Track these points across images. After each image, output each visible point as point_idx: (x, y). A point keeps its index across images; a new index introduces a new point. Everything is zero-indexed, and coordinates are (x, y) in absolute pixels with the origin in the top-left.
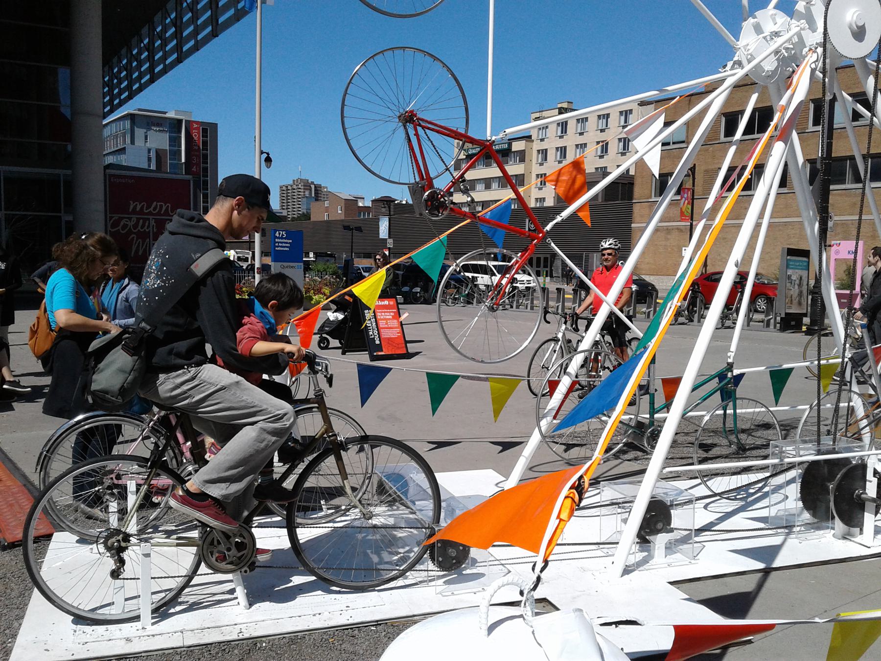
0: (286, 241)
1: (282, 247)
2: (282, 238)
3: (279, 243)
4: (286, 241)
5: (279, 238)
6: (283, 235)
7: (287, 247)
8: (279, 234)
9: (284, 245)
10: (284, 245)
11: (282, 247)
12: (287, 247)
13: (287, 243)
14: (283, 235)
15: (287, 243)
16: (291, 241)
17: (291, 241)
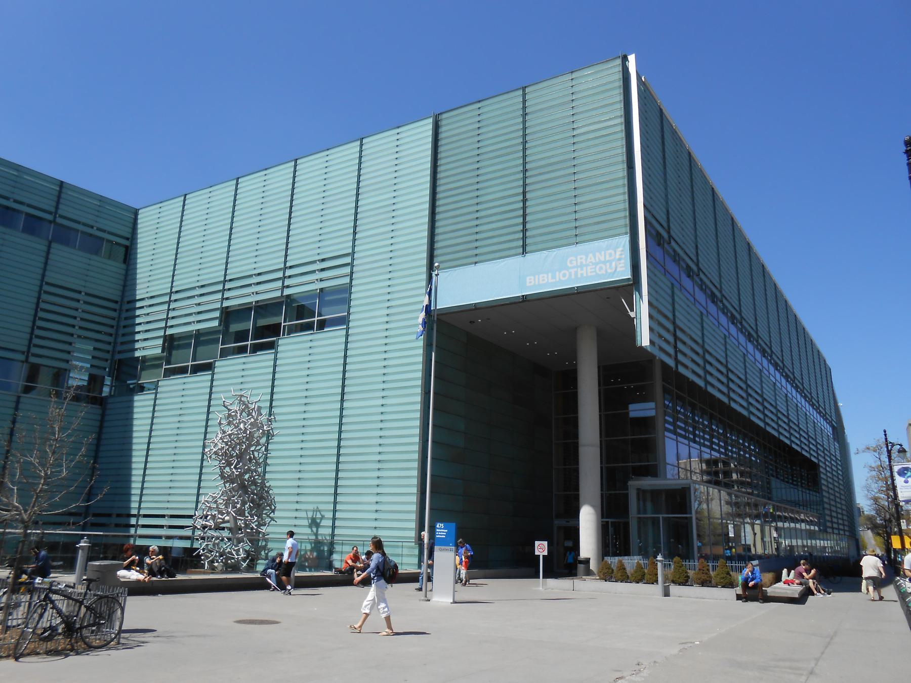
0: (443, 531)
1: (440, 535)
2: (441, 529)
3: (439, 532)
4: (443, 531)
5: (439, 529)
6: (441, 526)
7: (444, 535)
8: (439, 525)
9: (442, 533)
10: (442, 533)
11: (440, 535)
12: (444, 535)
13: (444, 532)
14: (441, 526)
15: (444, 532)
16: (447, 531)
17: (447, 531)
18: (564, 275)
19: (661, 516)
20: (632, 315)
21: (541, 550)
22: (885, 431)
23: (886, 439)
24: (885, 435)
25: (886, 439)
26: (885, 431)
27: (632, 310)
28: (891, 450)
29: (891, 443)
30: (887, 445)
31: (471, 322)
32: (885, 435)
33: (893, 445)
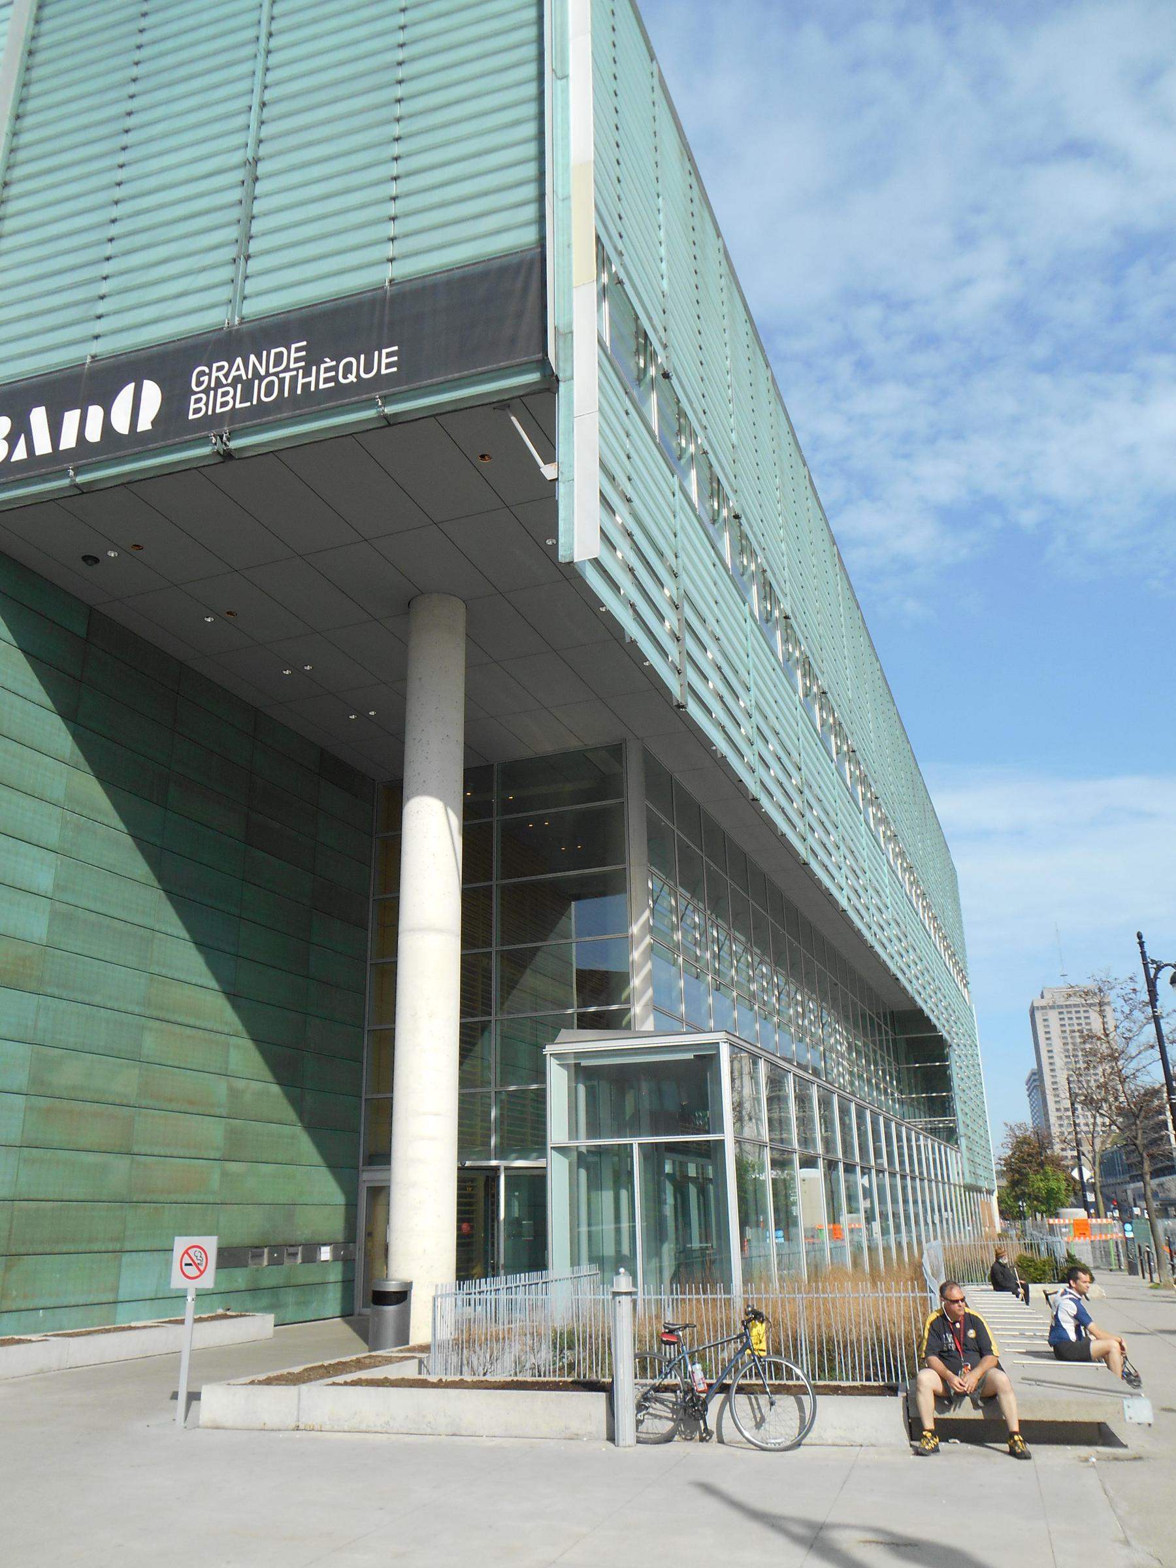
18: (348, 369)
19: (635, 1142)
20: (549, 471)
21: (192, 1271)
22: (1140, 936)
23: (1143, 953)
24: (1141, 944)
25: (1143, 953)
26: (1140, 936)
27: (550, 457)
28: (1156, 977)
29: (1153, 962)
30: (1145, 965)
31: (86, 558)
32: (1141, 944)
33: (1159, 968)
